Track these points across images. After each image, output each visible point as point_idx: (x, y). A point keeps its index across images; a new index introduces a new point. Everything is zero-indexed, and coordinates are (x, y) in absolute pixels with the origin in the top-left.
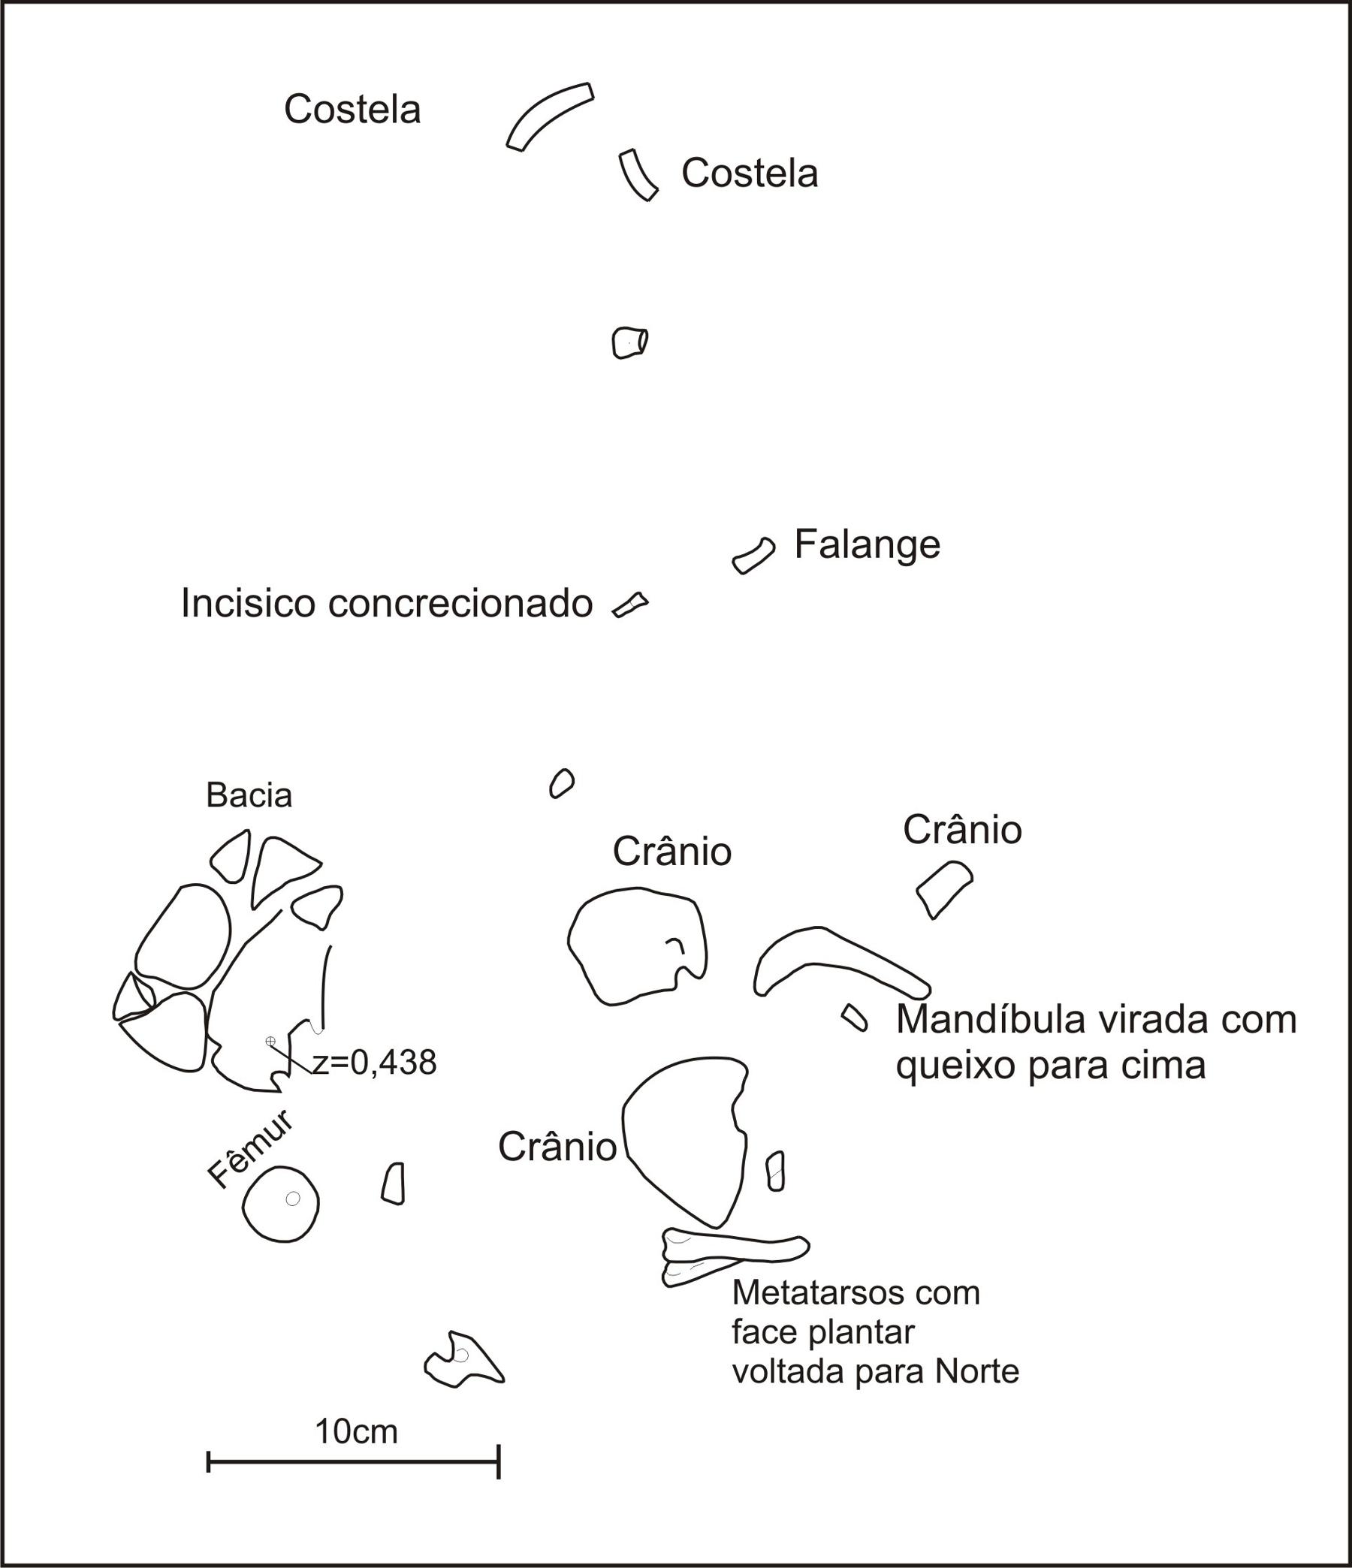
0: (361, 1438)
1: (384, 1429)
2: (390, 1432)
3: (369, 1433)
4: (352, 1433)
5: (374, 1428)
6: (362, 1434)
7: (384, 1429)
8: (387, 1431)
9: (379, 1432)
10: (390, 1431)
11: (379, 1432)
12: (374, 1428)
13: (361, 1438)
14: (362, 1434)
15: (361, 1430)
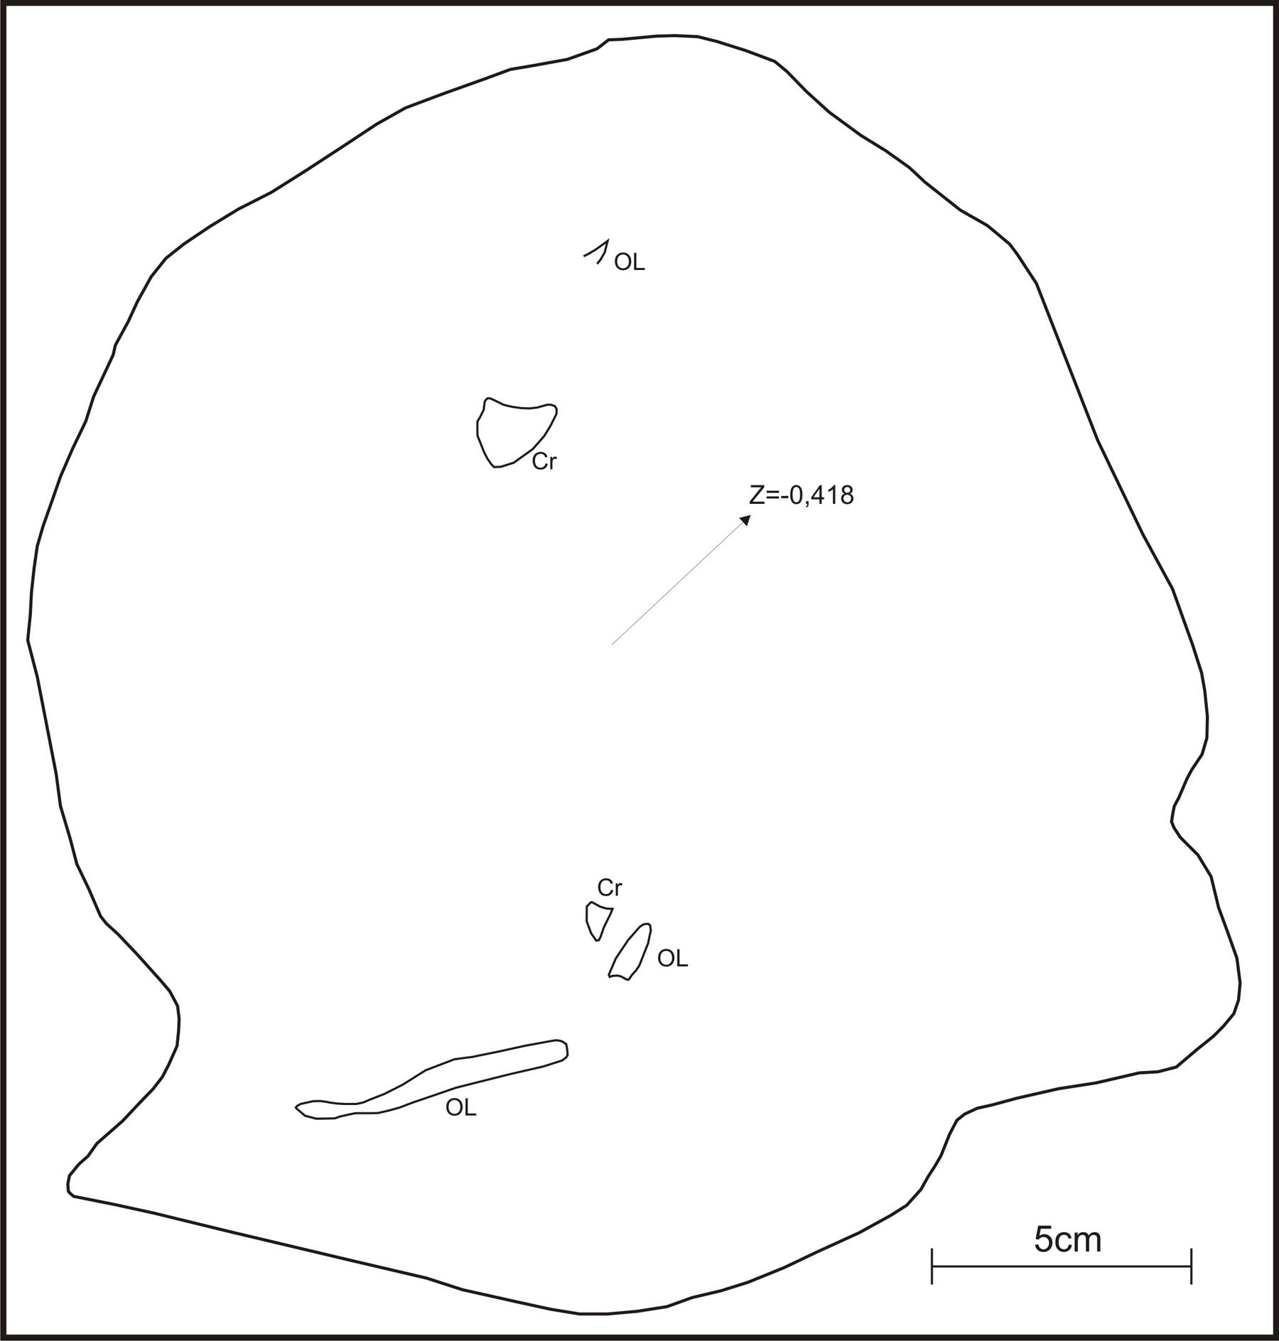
0: (1063, 1245)
1: (1088, 1237)
2: (1093, 1239)
3: (1072, 1242)
4: (1054, 1243)
5: (1077, 1236)
6: (1064, 1242)
7: (1088, 1237)
8: (1091, 1238)
9: (1082, 1239)
10: (1093, 1239)
11: (1082, 1239)
12: (1077, 1236)
13: (1063, 1245)
14: (1064, 1242)
15: (1063, 1238)
